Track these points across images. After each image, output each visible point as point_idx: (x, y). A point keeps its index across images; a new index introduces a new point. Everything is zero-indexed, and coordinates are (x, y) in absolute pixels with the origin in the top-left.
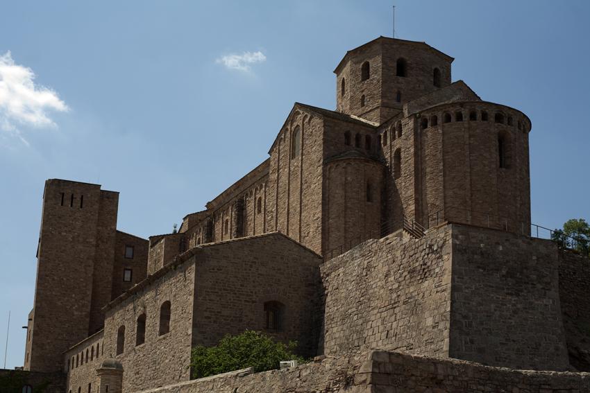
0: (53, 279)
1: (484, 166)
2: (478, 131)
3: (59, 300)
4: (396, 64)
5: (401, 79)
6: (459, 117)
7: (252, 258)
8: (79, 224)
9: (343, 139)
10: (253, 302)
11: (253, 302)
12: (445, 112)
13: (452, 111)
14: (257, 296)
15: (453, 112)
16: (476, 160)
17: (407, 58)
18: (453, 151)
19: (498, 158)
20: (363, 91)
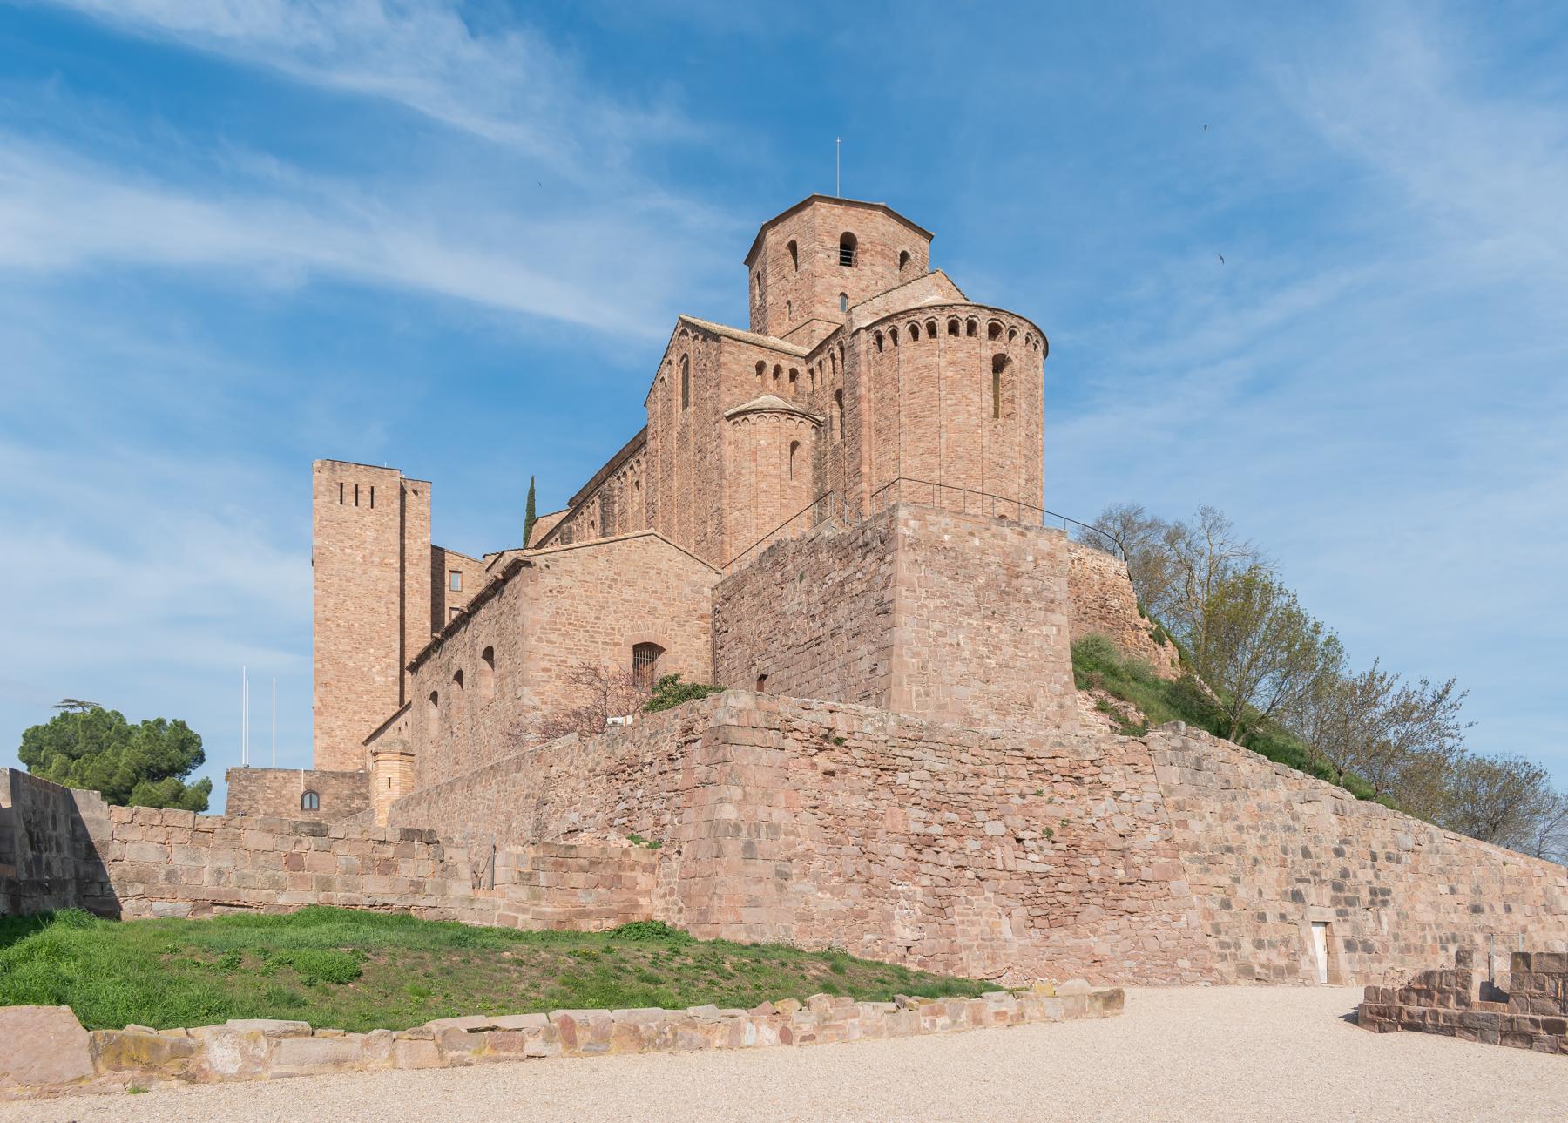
0: (338, 625)
1: (970, 415)
3: (351, 657)
7: (611, 573)
8: (371, 534)
10: (616, 644)
11: (616, 644)
12: (909, 322)
13: (921, 319)
14: (622, 635)
16: (956, 405)
18: (921, 390)
19: (992, 401)
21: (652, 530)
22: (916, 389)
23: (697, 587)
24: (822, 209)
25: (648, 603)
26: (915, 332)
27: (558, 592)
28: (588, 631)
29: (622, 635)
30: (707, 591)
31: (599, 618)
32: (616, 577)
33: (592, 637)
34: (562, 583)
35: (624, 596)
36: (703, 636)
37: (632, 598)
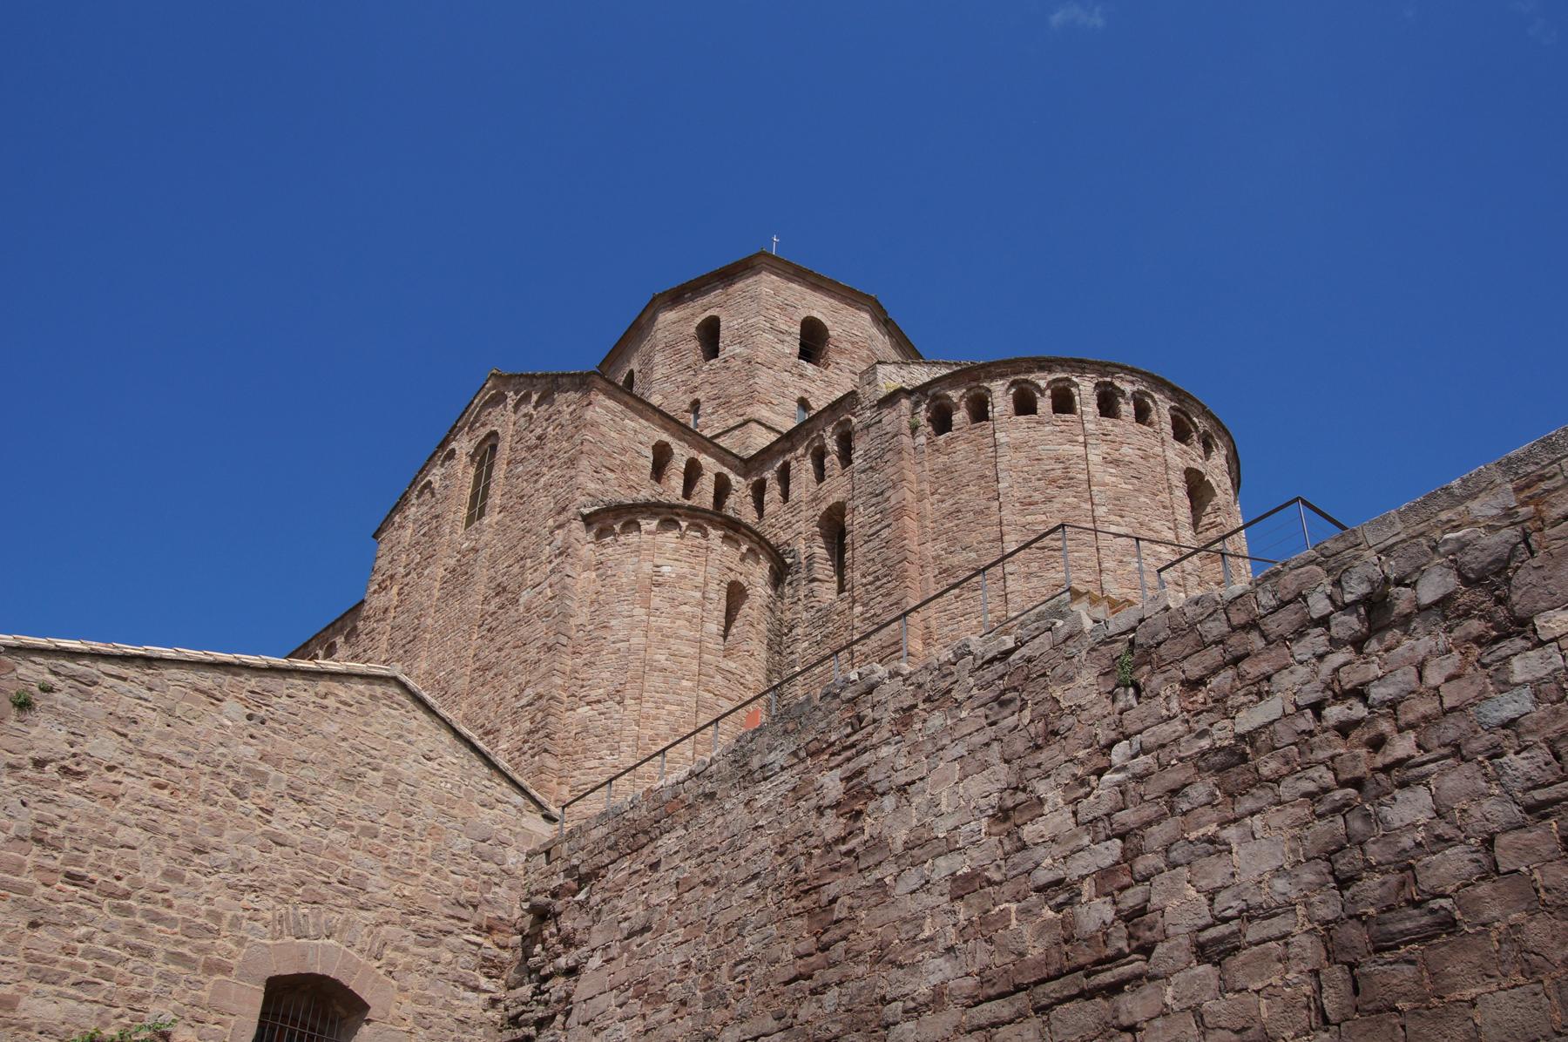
2: (1125, 449)
4: (797, 329)
5: (810, 369)
6: (1064, 402)
9: (647, 463)
15: (1043, 384)
17: (828, 324)
18: (1050, 500)
20: (694, 390)
21: (396, 670)
22: (1037, 496)
23: (486, 845)
24: (766, 284)
25: (344, 858)
26: (1025, 405)
27: (65, 771)
28: (128, 911)
29: (240, 942)
30: (514, 859)
31: (179, 878)
32: (263, 767)
33: (138, 929)
34: (90, 745)
35: (276, 825)
36: (484, 982)
37: (296, 837)
